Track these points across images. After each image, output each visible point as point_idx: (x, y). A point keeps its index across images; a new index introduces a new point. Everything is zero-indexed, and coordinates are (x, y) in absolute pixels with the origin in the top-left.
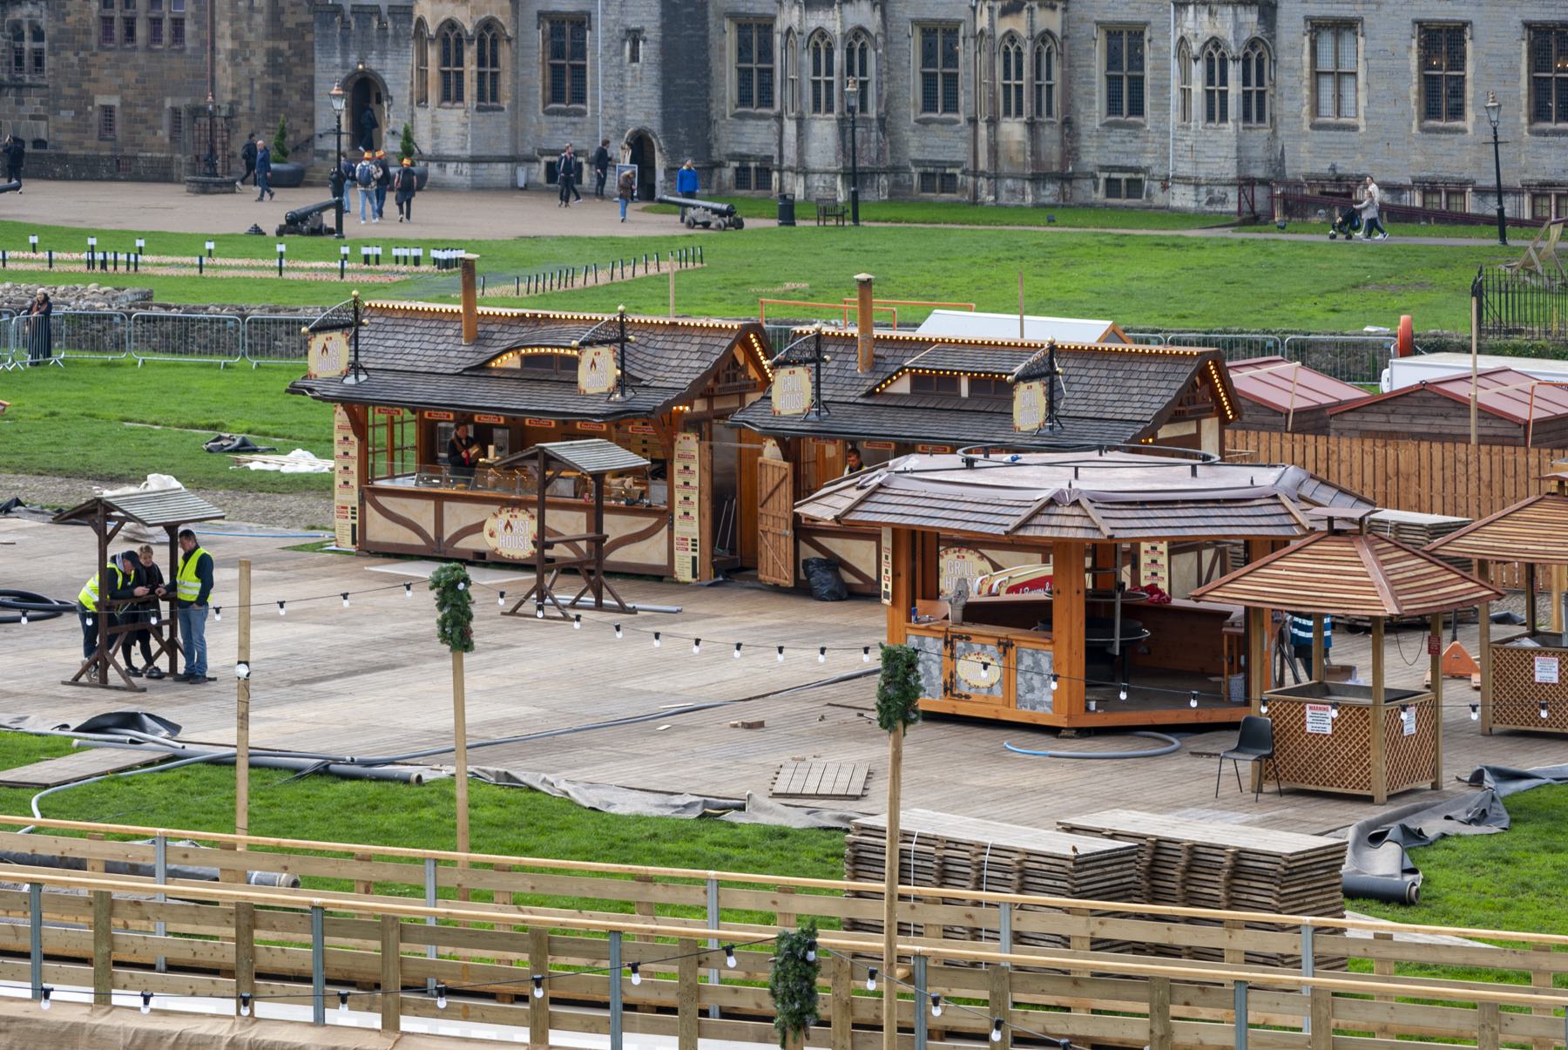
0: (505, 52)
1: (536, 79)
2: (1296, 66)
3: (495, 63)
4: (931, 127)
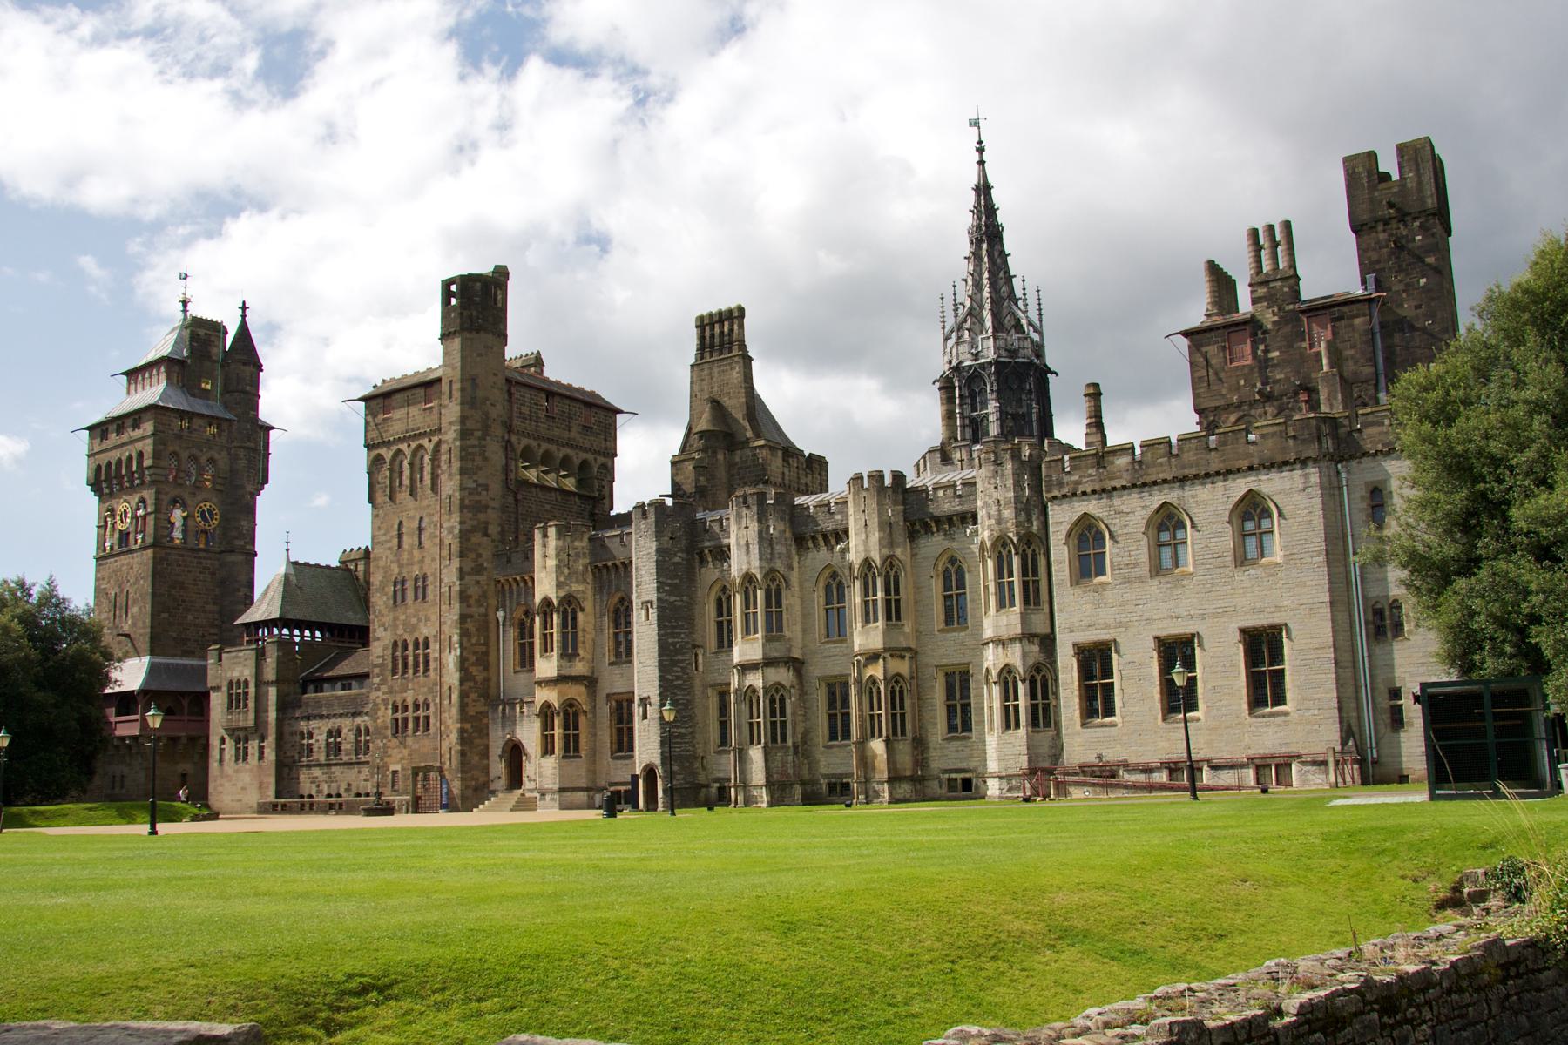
0: (582, 720)
1: (606, 736)
2: (1069, 681)
3: (576, 728)
4: (835, 750)
